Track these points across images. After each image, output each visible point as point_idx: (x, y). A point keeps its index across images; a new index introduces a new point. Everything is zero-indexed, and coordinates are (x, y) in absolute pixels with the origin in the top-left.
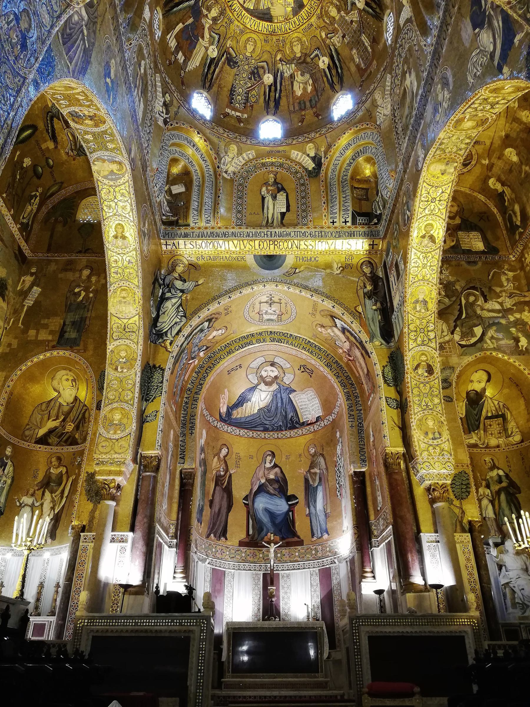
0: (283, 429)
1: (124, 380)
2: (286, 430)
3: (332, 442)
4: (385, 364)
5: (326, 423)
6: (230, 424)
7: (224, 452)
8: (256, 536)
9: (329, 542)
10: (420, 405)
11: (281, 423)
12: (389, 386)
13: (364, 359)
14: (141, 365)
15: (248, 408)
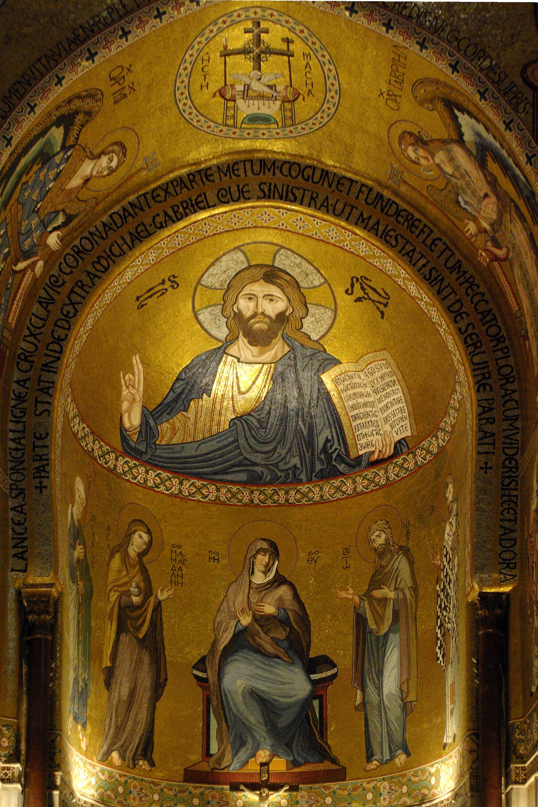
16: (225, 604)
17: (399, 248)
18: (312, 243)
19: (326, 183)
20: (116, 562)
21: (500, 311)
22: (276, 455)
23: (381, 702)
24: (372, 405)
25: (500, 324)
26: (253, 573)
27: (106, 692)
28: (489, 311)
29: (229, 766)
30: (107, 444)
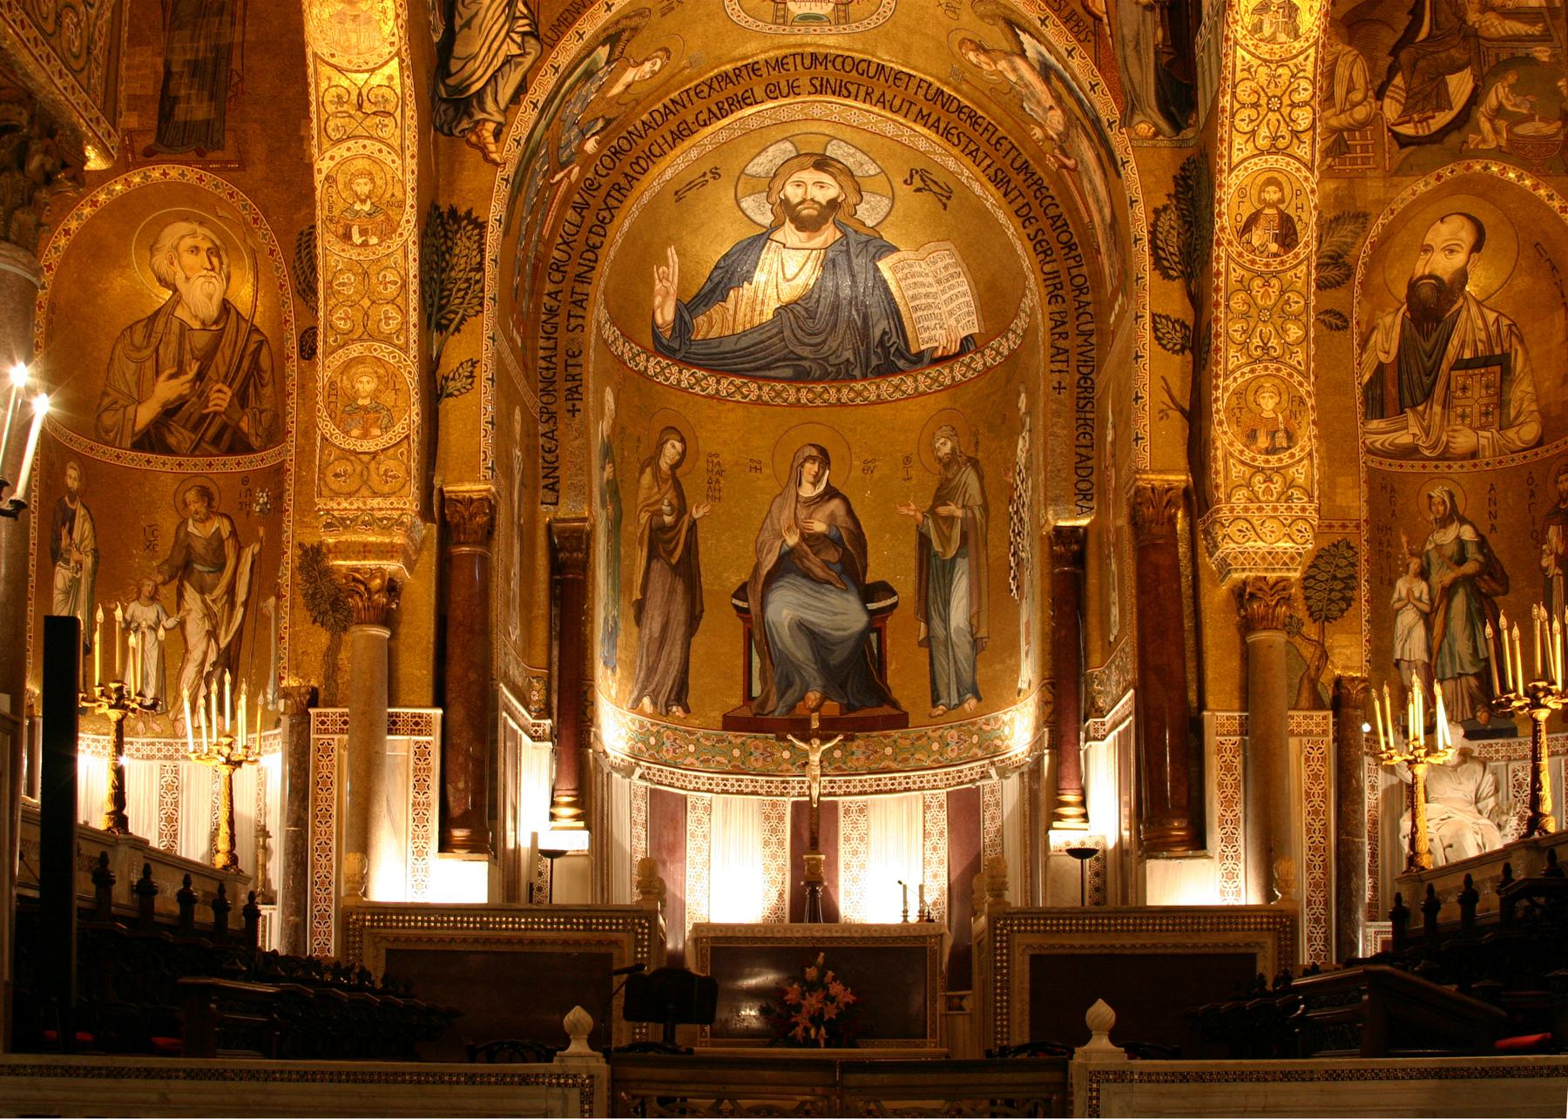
0: (857, 372)
1: (373, 270)
2: (864, 377)
3: (1005, 425)
4: (1161, 201)
5: (989, 361)
6: (687, 362)
7: (672, 449)
8: (773, 698)
9: (981, 720)
10: (1244, 346)
11: (848, 354)
12: (1166, 276)
13: (1106, 176)
14: (418, 221)
15: (743, 308)
16: (768, 521)
17: (961, 147)
18: (868, 135)
19: (882, 77)
20: (647, 478)
21: (1071, 217)
22: (826, 348)
23: (948, 637)
24: (935, 295)
25: (1071, 230)
26: (800, 484)
27: (635, 630)
28: (1060, 216)
29: (773, 711)
30: (637, 344)
